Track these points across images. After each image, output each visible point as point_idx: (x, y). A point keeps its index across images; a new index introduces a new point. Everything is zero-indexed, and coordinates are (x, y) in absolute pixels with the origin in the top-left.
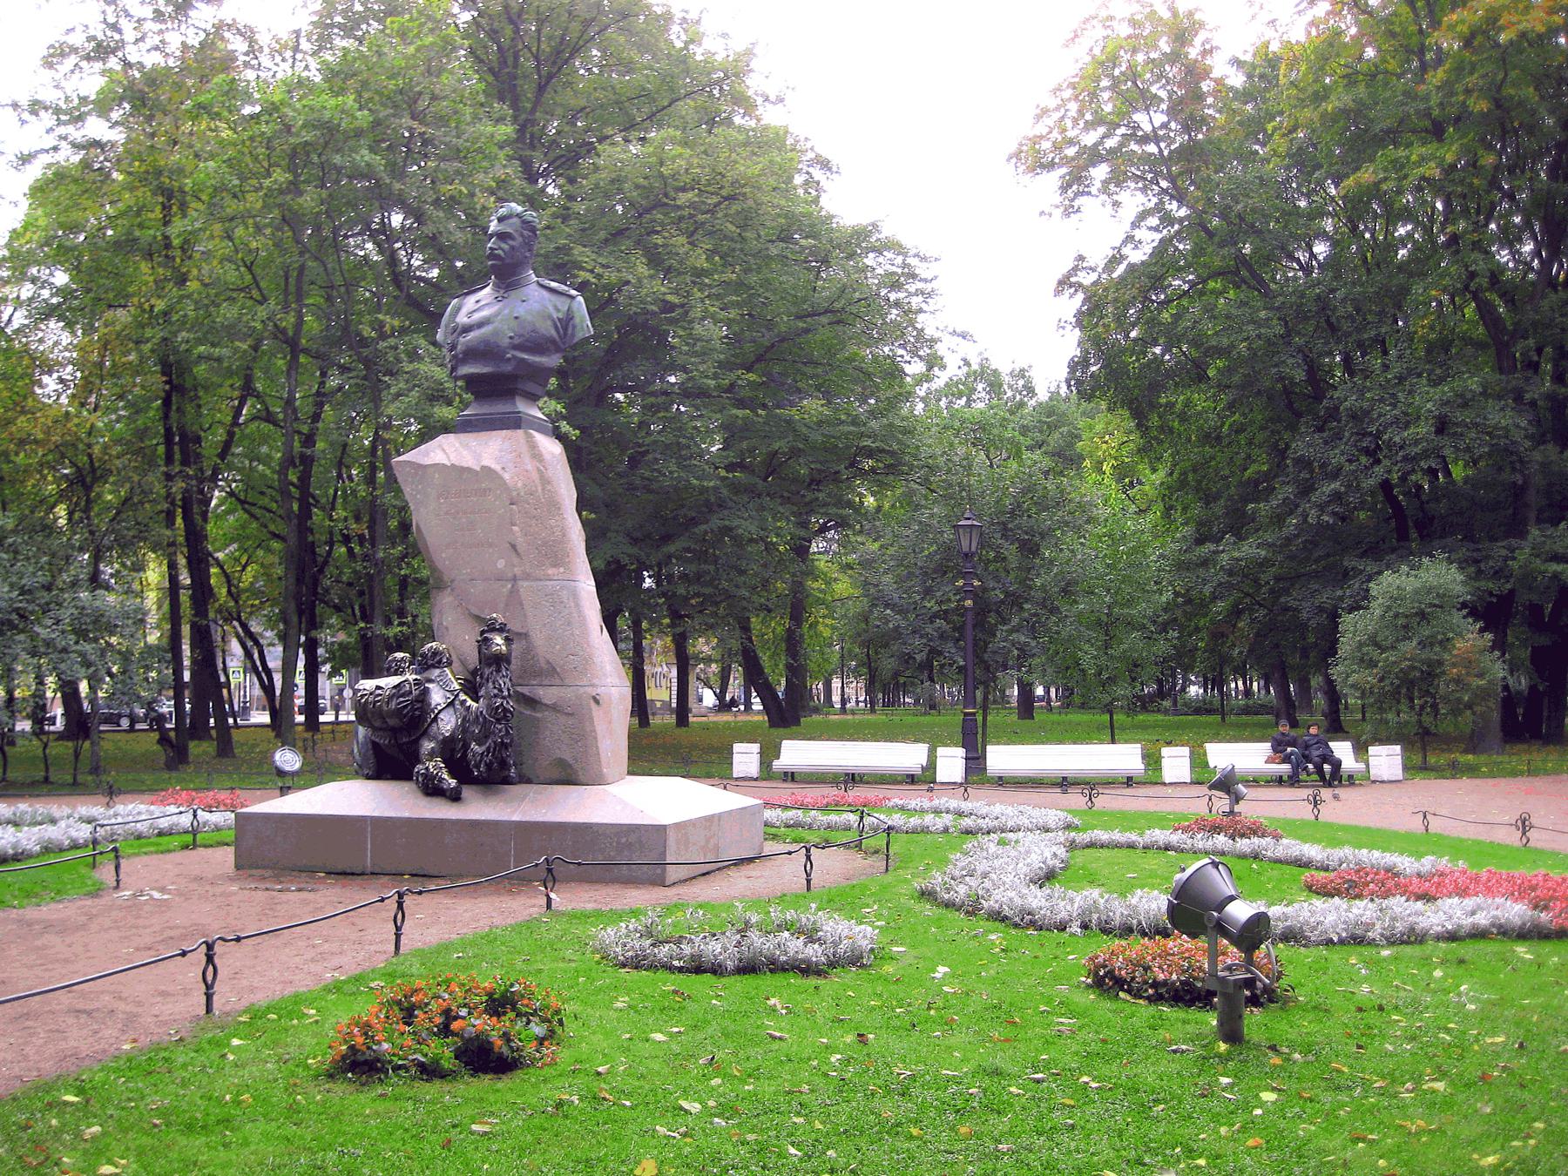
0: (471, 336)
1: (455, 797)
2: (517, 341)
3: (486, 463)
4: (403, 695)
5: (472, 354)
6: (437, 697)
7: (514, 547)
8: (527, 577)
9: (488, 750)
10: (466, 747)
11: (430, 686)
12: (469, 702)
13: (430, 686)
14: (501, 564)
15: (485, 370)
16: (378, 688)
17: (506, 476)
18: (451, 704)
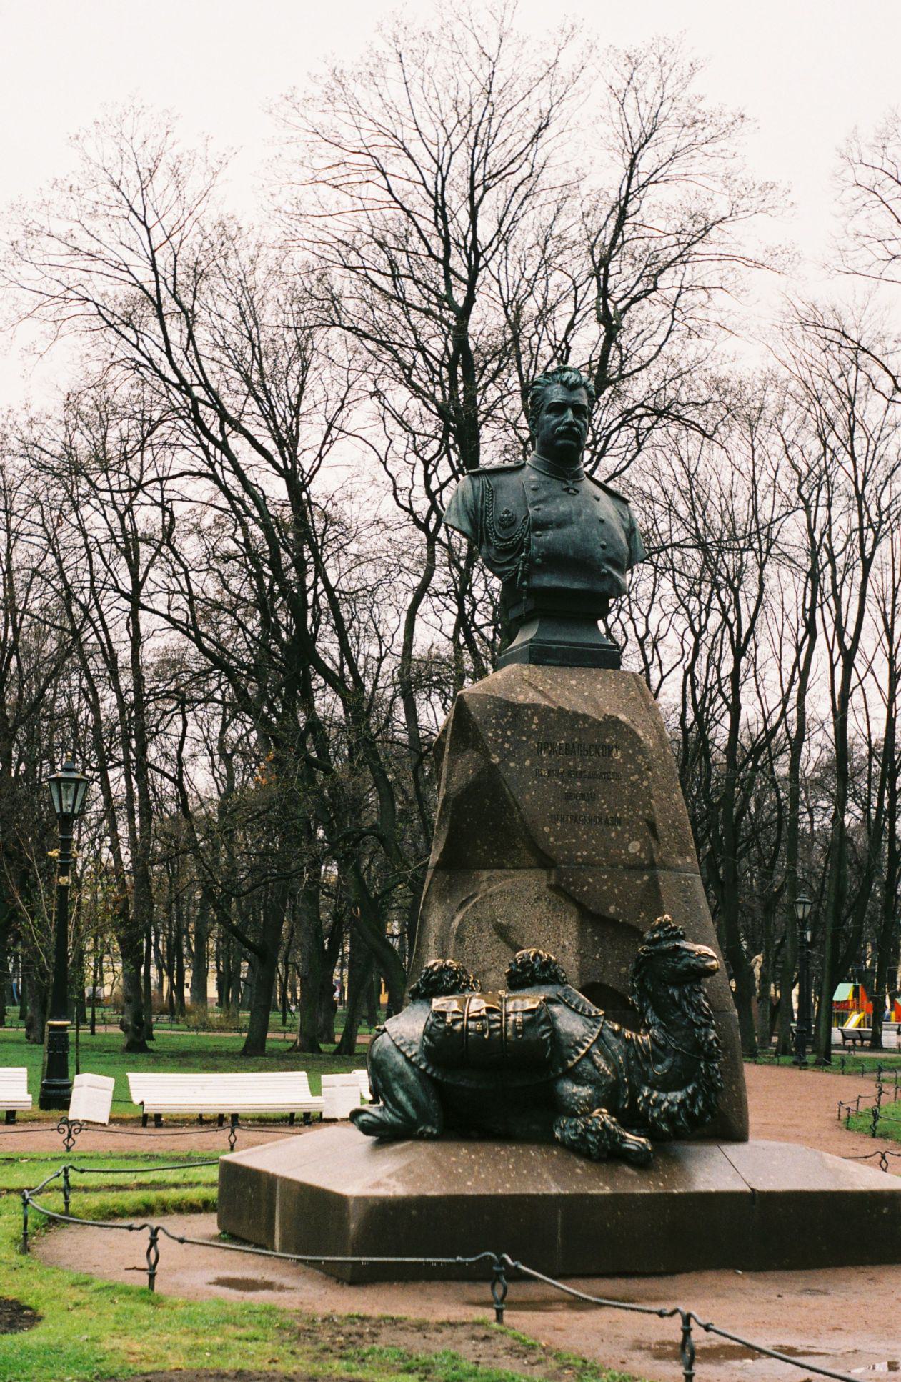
0: (550, 535)
1: (641, 1162)
2: (611, 554)
3: (609, 711)
4: (543, 1023)
5: (555, 560)
6: (570, 1024)
7: (652, 826)
8: (664, 866)
9: (692, 1098)
10: (636, 1092)
11: (556, 1009)
12: (628, 1034)
13: (556, 1009)
14: (634, 847)
15: (577, 586)
16: (489, 1010)
17: (640, 733)
18: (601, 1034)
